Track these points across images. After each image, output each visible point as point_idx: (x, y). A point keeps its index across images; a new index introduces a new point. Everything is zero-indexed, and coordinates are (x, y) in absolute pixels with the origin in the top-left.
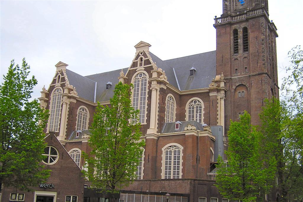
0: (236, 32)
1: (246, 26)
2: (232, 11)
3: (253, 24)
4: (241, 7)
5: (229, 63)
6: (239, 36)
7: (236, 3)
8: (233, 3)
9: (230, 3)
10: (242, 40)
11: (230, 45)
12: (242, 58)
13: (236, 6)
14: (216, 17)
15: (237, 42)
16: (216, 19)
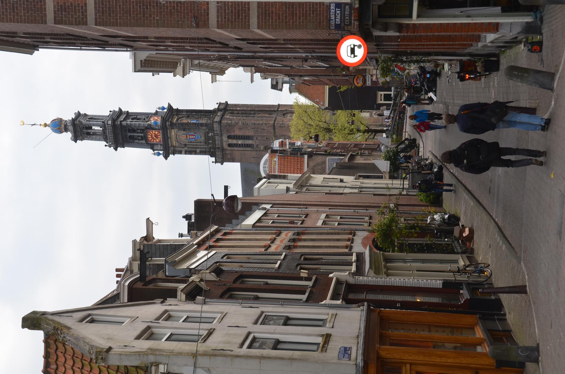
0: (230, 145)
1: (227, 136)
2: (206, 146)
3: (227, 131)
4: (203, 138)
5: (261, 152)
6: (235, 143)
7: (198, 143)
8: (199, 145)
9: (198, 148)
10: (239, 141)
11: (243, 151)
12: (257, 141)
13: (201, 143)
14: (213, 162)
15: (240, 144)
16: (216, 162)
